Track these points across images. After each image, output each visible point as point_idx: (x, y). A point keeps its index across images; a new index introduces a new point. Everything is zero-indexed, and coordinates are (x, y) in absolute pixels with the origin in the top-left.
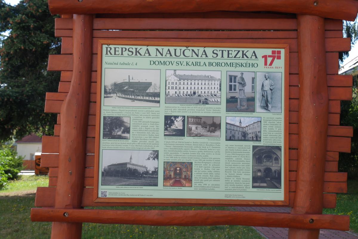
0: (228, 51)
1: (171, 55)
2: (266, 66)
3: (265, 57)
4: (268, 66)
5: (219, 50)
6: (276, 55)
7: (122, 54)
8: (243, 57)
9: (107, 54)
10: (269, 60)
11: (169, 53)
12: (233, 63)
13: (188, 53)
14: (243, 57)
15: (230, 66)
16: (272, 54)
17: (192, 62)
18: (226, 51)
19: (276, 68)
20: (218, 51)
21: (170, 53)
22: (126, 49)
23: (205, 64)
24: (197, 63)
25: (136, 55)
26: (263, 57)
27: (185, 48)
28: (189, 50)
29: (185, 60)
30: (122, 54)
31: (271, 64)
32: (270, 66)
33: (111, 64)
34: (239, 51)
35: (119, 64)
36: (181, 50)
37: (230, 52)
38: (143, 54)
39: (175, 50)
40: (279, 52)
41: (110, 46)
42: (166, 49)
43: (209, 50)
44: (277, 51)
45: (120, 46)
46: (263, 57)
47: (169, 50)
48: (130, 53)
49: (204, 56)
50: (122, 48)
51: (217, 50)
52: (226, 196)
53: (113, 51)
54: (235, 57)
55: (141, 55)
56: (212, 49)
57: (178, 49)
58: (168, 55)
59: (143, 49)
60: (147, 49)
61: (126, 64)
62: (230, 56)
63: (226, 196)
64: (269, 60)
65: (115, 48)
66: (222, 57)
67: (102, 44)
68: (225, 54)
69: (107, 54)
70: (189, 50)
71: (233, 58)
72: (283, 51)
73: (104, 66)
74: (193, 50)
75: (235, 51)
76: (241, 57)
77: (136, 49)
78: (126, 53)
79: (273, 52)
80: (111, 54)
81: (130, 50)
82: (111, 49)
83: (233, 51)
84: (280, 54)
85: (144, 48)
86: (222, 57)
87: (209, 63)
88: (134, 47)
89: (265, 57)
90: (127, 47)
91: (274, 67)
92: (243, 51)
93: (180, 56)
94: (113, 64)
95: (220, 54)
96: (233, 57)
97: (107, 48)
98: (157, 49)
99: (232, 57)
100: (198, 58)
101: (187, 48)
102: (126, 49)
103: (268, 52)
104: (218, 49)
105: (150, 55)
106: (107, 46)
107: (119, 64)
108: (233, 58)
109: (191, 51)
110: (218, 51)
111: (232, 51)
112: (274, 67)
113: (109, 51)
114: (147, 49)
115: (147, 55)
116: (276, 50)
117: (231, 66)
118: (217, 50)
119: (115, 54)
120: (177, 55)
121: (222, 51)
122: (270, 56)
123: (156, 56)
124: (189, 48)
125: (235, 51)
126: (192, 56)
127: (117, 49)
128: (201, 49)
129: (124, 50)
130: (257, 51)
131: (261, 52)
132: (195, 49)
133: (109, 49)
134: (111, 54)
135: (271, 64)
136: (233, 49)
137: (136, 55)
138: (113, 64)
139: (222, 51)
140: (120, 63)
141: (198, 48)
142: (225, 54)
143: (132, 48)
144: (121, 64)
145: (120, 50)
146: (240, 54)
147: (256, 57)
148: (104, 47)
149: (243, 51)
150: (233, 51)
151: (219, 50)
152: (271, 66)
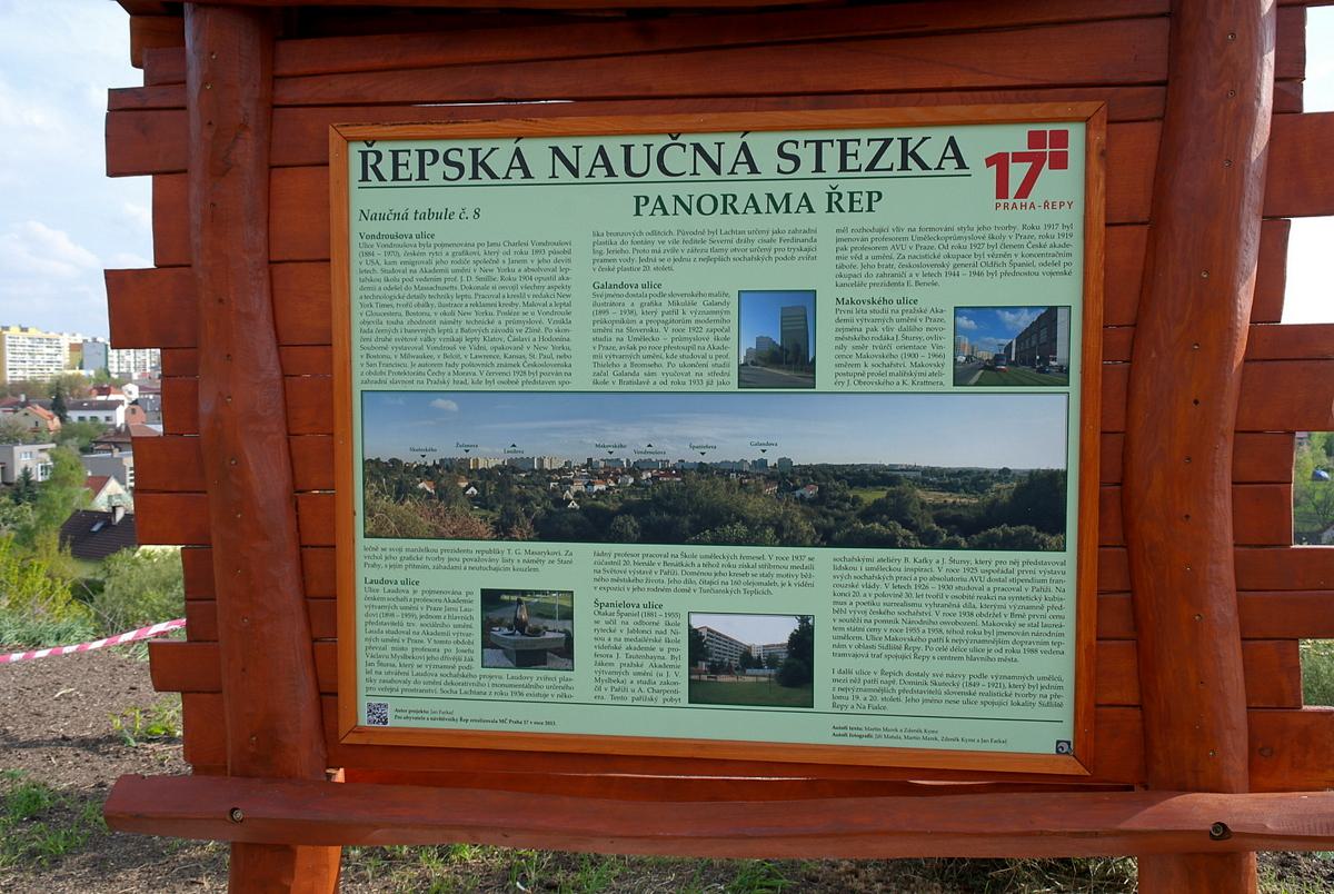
0: (844, 143)
1: (611, 173)
2: (1002, 201)
3: (999, 161)
4: (1011, 200)
5: (806, 142)
6: (1048, 150)
7: (422, 177)
8: (904, 167)
9: (365, 178)
10: (1017, 172)
11: (519, 165)
12: (852, 194)
13: (678, 159)
14: (904, 167)
15: (783, 208)
16: (1029, 148)
17: (752, 197)
18: (832, 141)
19: (1046, 205)
20: (801, 144)
21: (607, 165)
22: (435, 153)
23: (662, 203)
24: (835, 197)
25: (475, 176)
26: (989, 162)
27: (667, 140)
28: (684, 146)
29: (667, 192)
30: (422, 177)
31: (1024, 191)
32: (1018, 201)
33: (382, 217)
34: (887, 142)
35: (411, 216)
36: (649, 146)
37: (851, 148)
38: (500, 173)
39: (627, 148)
40: (1061, 139)
41: (376, 147)
42: (590, 146)
43: (764, 145)
44: (1051, 132)
45: (414, 146)
46: (989, 162)
47: (601, 151)
48: (454, 172)
49: (743, 170)
50: (422, 153)
51: (796, 143)
52: (837, 732)
53: (386, 167)
54: (871, 168)
55: (493, 176)
56: (776, 138)
57: (638, 143)
58: (601, 173)
59: (500, 155)
60: (518, 152)
61: (439, 217)
62: (851, 163)
63: (837, 732)
64: (1017, 172)
65: (395, 154)
66: (819, 168)
67: (349, 140)
68: (831, 155)
69: (365, 178)
70: (684, 146)
71: (863, 173)
72: (1076, 133)
73: (358, 227)
74: (698, 147)
75: (869, 140)
76: (898, 165)
77: (475, 152)
78: (435, 172)
79: (1036, 140)
80: (381, 178)
81: (453, 156)
82: (379, 156)
83: (864, 142)
84: (1066, 147)
85: (507, 148)
86: (819, 168)
87: (638, 198)
88: (466, 145)
89: (999, 161)
90: (441, 147)
91: (1039, 202)
92: (905, 142)
93: (646, 173)
94: (391, 217)
95: (807, 155)
96: (863, 168)
97: (365, 154)
98: (556, 151)
99: (859, 170)
100: (718, 178)
101: (673, 138)
102: (435, 153)
103: (1014, 138)
104: (801, 137)
105: (527, 175)
106: (364, 147)
107: (411, 216)
108: (863, 173)
109: (690, 149)
110: (801, 144)
111: (859, 141)
112: (1039, 202)
113: (374, 167)
114: (518, 152)
115: (517, 174)
116: (1048, 128)
117: (788, 211)
118: (796, 143)
119: (396, 178)
120: (634, 169)
121: (819, 144)
122: (1019, 157)
123: (554, 176)
124: (681, 140)
125: (869, 140)
126: (695, 173)
127: (402, 158)
128: (732, 142)
129: (429, 157)
130: (968, 138)
131: (980, 142)
132: (708, 141)
133: (372, 159)
134: (381, 178)
135: (1024, 191)
136: (864, 135)
137: (475, 176)
138: (391, 217)
139: (819, 144)
140: (416, 213)
141: (719, 138)
142: (831, 155)
143: (461, 151)
144: (418, 216)
145: (414, 160)
146: (893, 155)
147: (962, 165)
148: (355, 150)
149: (905, 142)
150: (864, 142)
151: (806, 142)
152: (1024, 201)
